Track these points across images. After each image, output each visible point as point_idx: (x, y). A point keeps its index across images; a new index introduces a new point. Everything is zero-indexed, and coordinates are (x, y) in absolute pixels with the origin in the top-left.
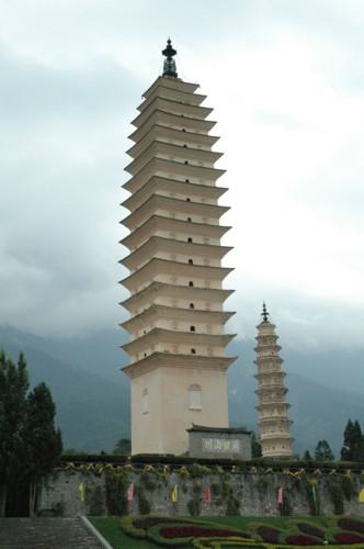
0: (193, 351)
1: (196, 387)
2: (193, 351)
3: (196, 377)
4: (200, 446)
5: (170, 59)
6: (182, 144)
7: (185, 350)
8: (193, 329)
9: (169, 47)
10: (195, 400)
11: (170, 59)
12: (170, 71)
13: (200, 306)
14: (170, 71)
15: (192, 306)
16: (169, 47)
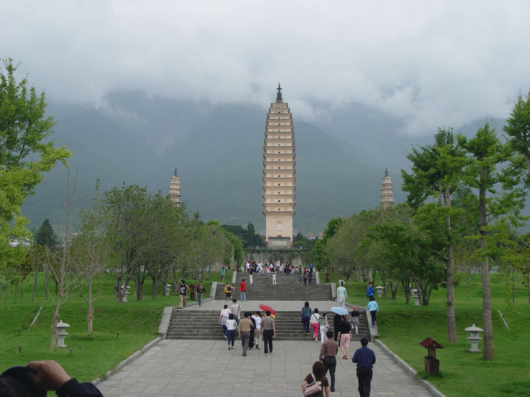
0: (279, 209)
1: (280, 222)
2: (279, 209)
3: (280, 218)
4: (271, 243)
5: (279, 92)
6: (277, 130)
7: (276, 209)
8: (279, 201)
9: (279, 87)
10: (279, 227)
11: (279, 92)
12: (279, 97)
13: (283, 193)
14: (279, 97)
15: (279, 193)
16: (279, 87)
